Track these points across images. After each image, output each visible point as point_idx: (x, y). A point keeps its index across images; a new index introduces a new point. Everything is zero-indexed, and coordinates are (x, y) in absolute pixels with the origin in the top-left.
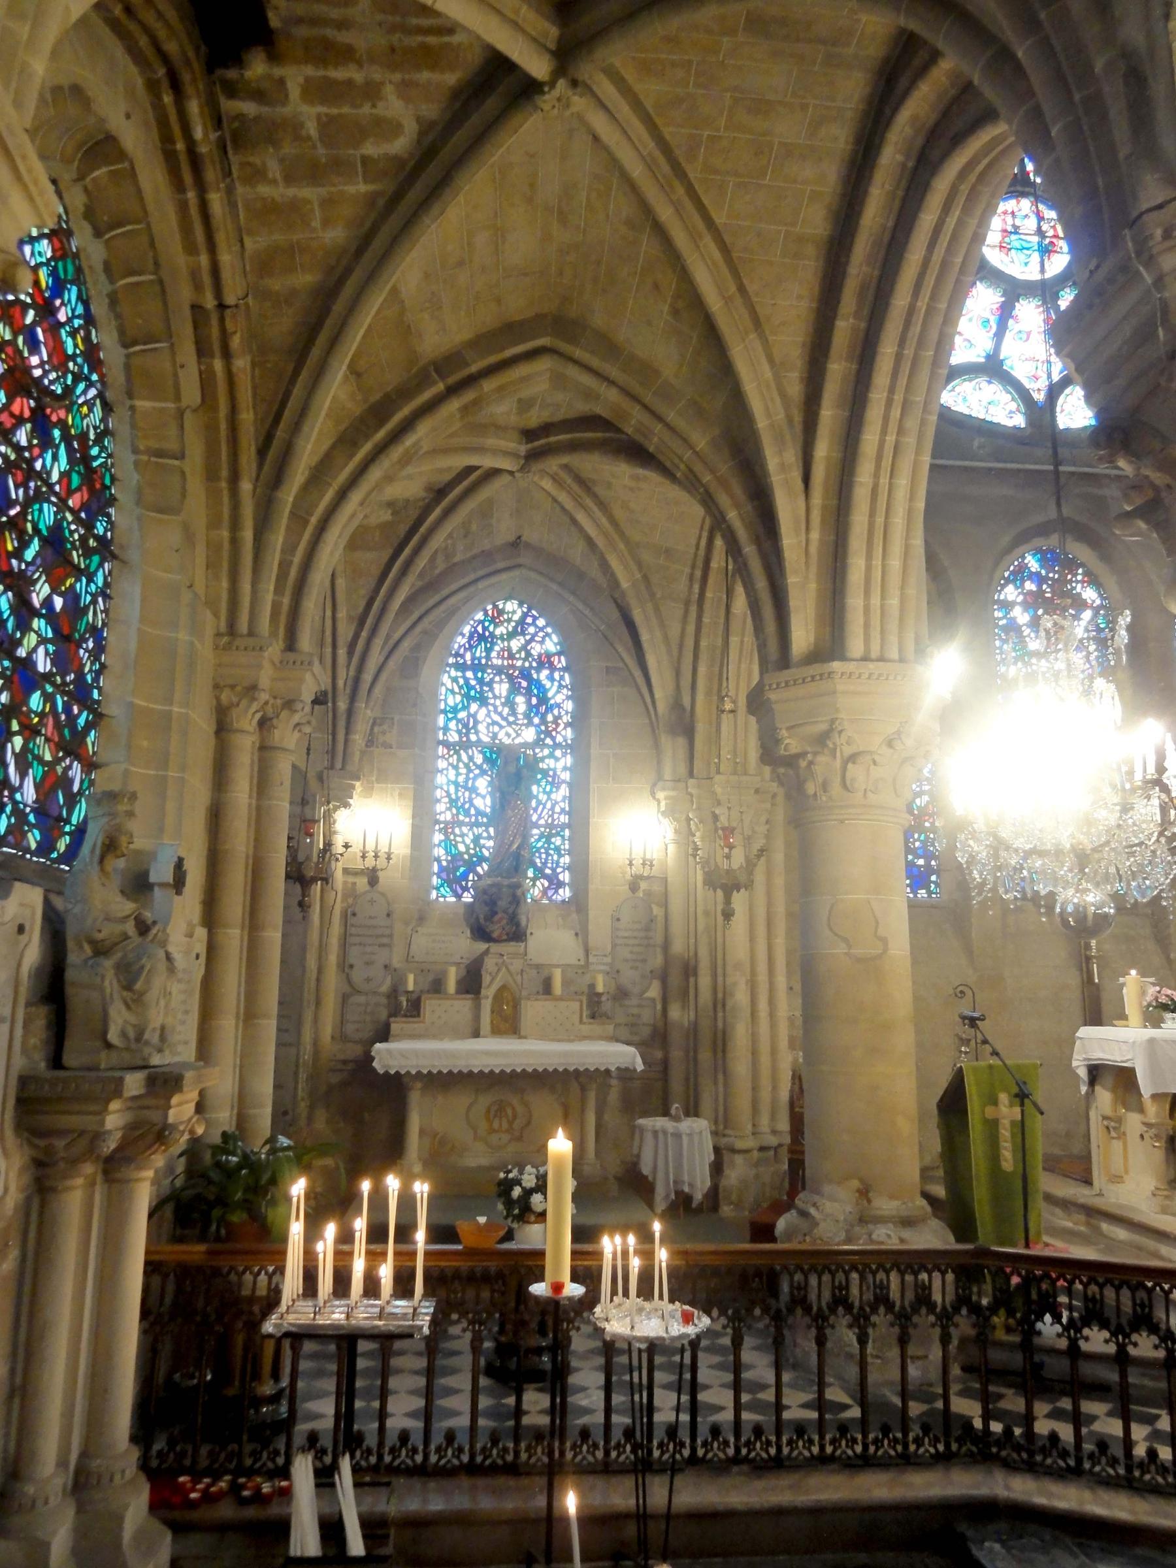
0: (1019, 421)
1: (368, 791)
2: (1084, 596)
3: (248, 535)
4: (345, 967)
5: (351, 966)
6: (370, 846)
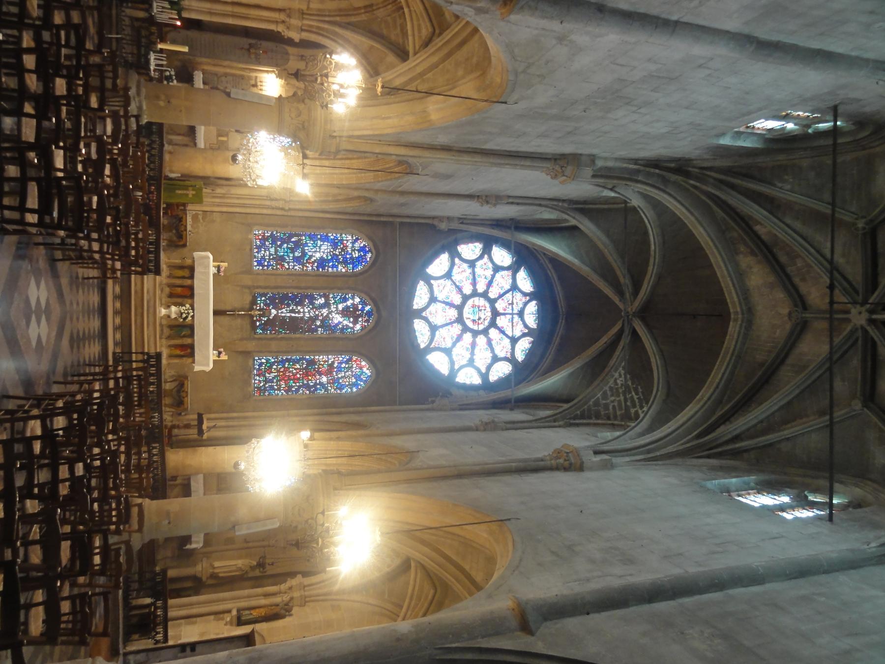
0: (415, 307)
1: (282, 86)
2: (358, 325)
3: (327, 19)
4: (226, 75)
5: (226, 77)
6: (264, 84)
